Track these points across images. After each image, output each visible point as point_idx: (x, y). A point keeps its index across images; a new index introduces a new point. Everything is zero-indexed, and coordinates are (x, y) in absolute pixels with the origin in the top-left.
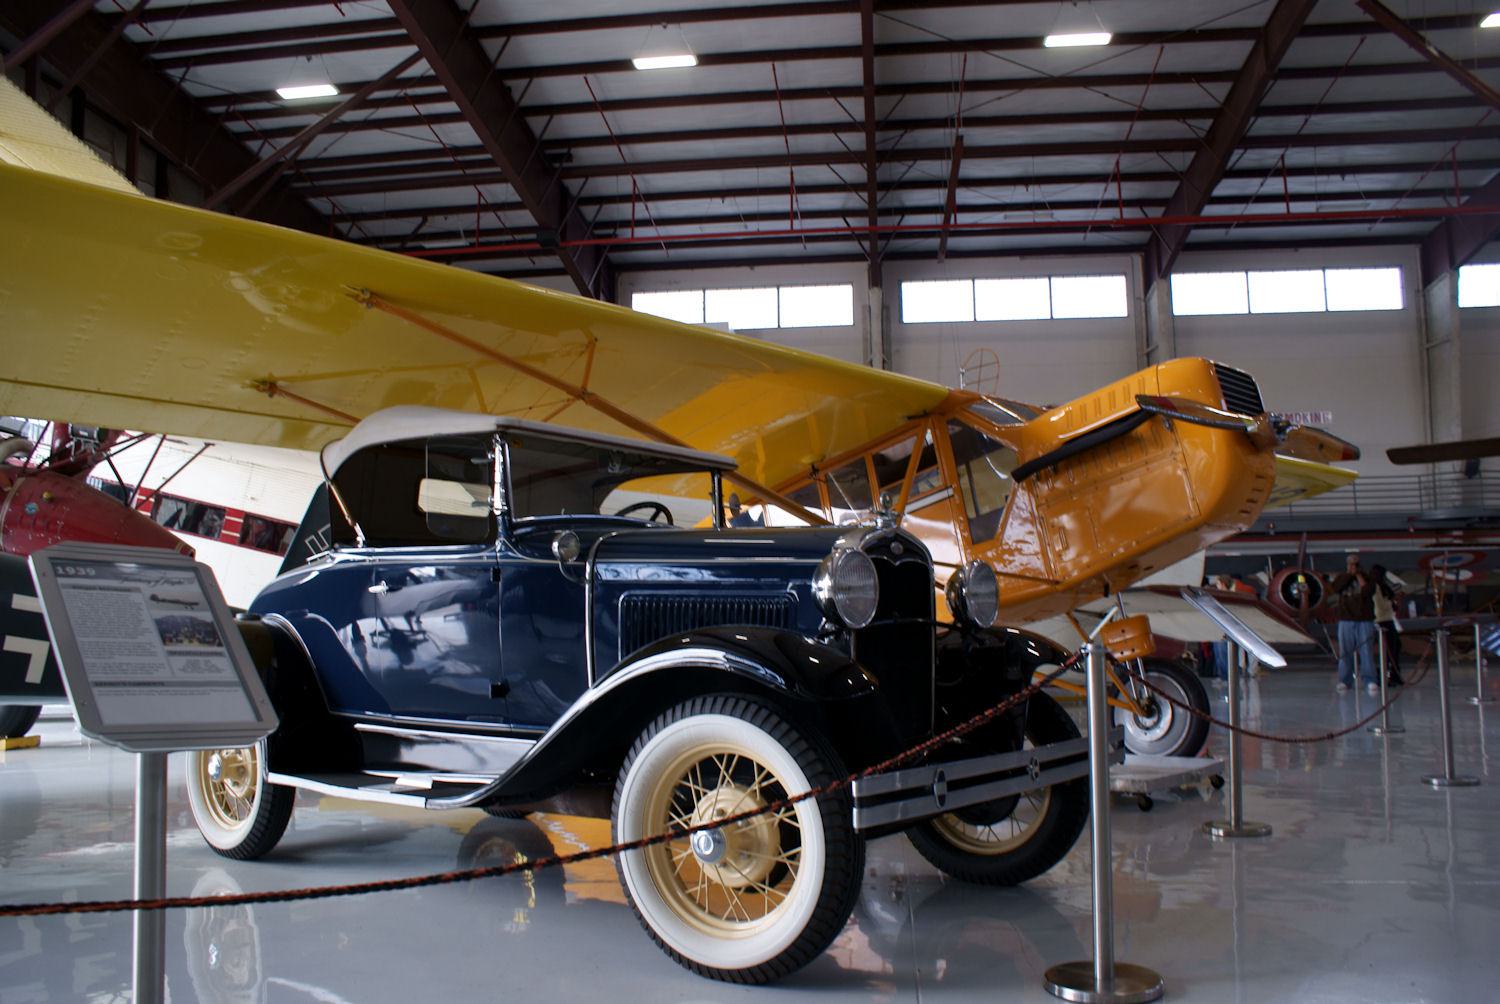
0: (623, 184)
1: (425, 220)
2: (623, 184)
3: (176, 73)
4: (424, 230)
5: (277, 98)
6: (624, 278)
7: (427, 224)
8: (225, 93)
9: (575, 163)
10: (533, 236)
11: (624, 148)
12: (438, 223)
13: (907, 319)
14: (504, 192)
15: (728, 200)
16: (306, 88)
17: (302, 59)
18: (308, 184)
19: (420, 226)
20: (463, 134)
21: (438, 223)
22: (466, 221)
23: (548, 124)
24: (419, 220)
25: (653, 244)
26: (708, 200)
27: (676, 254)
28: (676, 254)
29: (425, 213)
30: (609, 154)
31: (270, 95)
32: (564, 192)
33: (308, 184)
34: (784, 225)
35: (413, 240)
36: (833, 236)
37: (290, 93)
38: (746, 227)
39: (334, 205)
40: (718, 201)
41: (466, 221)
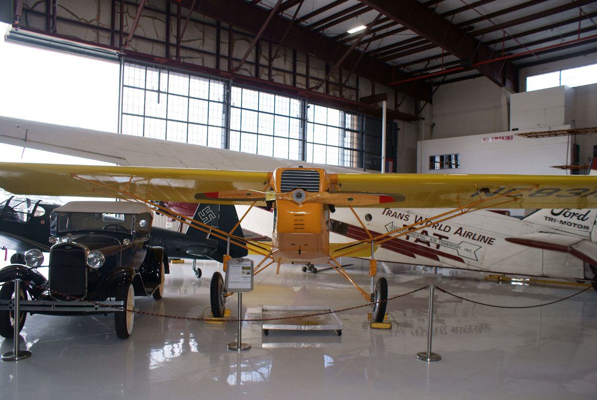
0: (499, 34)
1: (429, 62)
2: (499, 34)
3: (321, 32)
4: (429, 66)
5: (349, 34)
7: (430, 63)
8: (337, 35)
9: (475, 30)
10: (459, 64)
11: (492, 19)
12: (434, 62)
14: (438, 50)
15: (555, 29)
16: (357, 29)
17: (355, 18)
18: (381, 57)
19: (427, 65)
20: (409, 34)
21: (434, 62)
22: (439, 61)
23: (453, 18)
24: (427, 62)
25: (538, 53)
26: (545, 31)
27: (542, 56)
28: (542, 56)
29: (429, 59)
30: (485, 24)
31: (347, 34)
32: (477, 41)
33: (381, 57)
34: (575, 37)
35: (425, 71)
36: (575, 44)
37: (352, 31)
38: (564, 40)
39: (394, 63)
40: (549, 31)
41: (439, 61)
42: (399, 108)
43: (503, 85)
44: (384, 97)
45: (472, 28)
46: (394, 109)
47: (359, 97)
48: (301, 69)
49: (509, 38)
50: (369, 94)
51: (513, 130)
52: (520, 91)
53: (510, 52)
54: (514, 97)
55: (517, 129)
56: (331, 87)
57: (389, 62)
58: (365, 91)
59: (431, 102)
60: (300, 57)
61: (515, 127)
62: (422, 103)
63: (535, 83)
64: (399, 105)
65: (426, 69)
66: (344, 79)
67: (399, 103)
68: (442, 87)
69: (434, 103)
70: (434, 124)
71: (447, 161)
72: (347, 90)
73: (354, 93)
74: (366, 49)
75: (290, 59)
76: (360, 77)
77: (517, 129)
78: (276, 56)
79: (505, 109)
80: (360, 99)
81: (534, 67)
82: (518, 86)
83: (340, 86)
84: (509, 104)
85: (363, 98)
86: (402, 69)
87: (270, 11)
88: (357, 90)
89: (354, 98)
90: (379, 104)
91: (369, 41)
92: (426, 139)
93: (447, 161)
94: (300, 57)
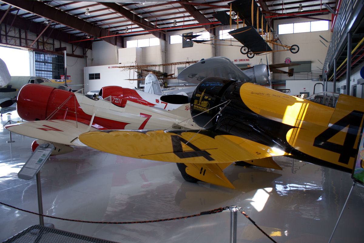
0: (108, 26)
6: (125, 38)
9: (98, 24)
11: (103, 22)
13: (171, 43)
42: (74, 53)
43: (116, 44)
44: (65, 49)
45: (97, 23)
46: (72, 53)
47: (55, 48)
48: (23, 36)
49: (112, 28)
50: (59, 47)
51: (120, 64)
52: (124, 47)
53: (118, 32)
54: (121, 50)
55: (121, 63)
56: (39, 44)
57: (67, 32)
58: (57, 45)
59: (91, 49)
60: (22, 31)
61: (120, 63)
62: (87, 49)
63: (131, 44)
64: (74, 52)
65: (85, 36)
66: (45, 40)
67: (74, 51)
68: (94, 42)
69: (93, 49)
70: (93, 59)
71: (97, 76)
72: (48, 45)
73: (52, 46)
74: (54, 27)
75: (17, 31)
76: (55, 40)
77: (121, 63)
78: (9, 31)
79: (116, 55)
80: (55, 49)
81: (129, 37)
82: (123, 46)
83: (44, 43)
84: (118, 52)
85: (57, 48)
86: (75, 35)
87: (6, 10)
88: (53, 44)
89: (52, 49)
90: (63, 51)
91: (55, 25)
92: (89, 66)
93: (97, 76)
94: (22, 31)
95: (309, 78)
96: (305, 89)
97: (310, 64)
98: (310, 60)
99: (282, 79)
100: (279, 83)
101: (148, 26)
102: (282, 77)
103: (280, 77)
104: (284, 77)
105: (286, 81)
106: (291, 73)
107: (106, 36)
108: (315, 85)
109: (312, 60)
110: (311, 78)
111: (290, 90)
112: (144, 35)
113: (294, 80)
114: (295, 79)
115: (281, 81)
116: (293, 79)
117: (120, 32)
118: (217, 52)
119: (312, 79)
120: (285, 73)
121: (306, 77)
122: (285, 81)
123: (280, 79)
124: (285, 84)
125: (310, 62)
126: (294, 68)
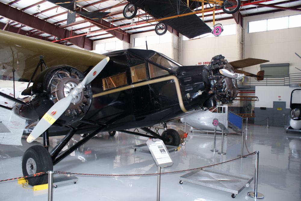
6: (94, 42)
95: (285, 84)
96: (280, 97)
97: (288, 67)
98: (288, 62)
99: (251, 84)
100: (248, 89)
101: (101, 24)
102: (251, 83)
103: (249, 82)
104: (253, 81)
105: (256, 87)
106: (260, 77)
107: (68, 37)
108: (292, 92)
109: (290, 63)
110: (288, 83)
111: (257, 97)
112: (111, 38)
113: (267, 85)
114: (268, 84)
115: (250, 87)
116: (266, 84)
117: (78, 32)
118: (180, 54)
119: (289, 85)
120: (252, 75)
121: (282, 82)
122: (254, 87)
123: (249, 84)
124: (254, 91)
125: (288, 65)
126: (265, 70)
